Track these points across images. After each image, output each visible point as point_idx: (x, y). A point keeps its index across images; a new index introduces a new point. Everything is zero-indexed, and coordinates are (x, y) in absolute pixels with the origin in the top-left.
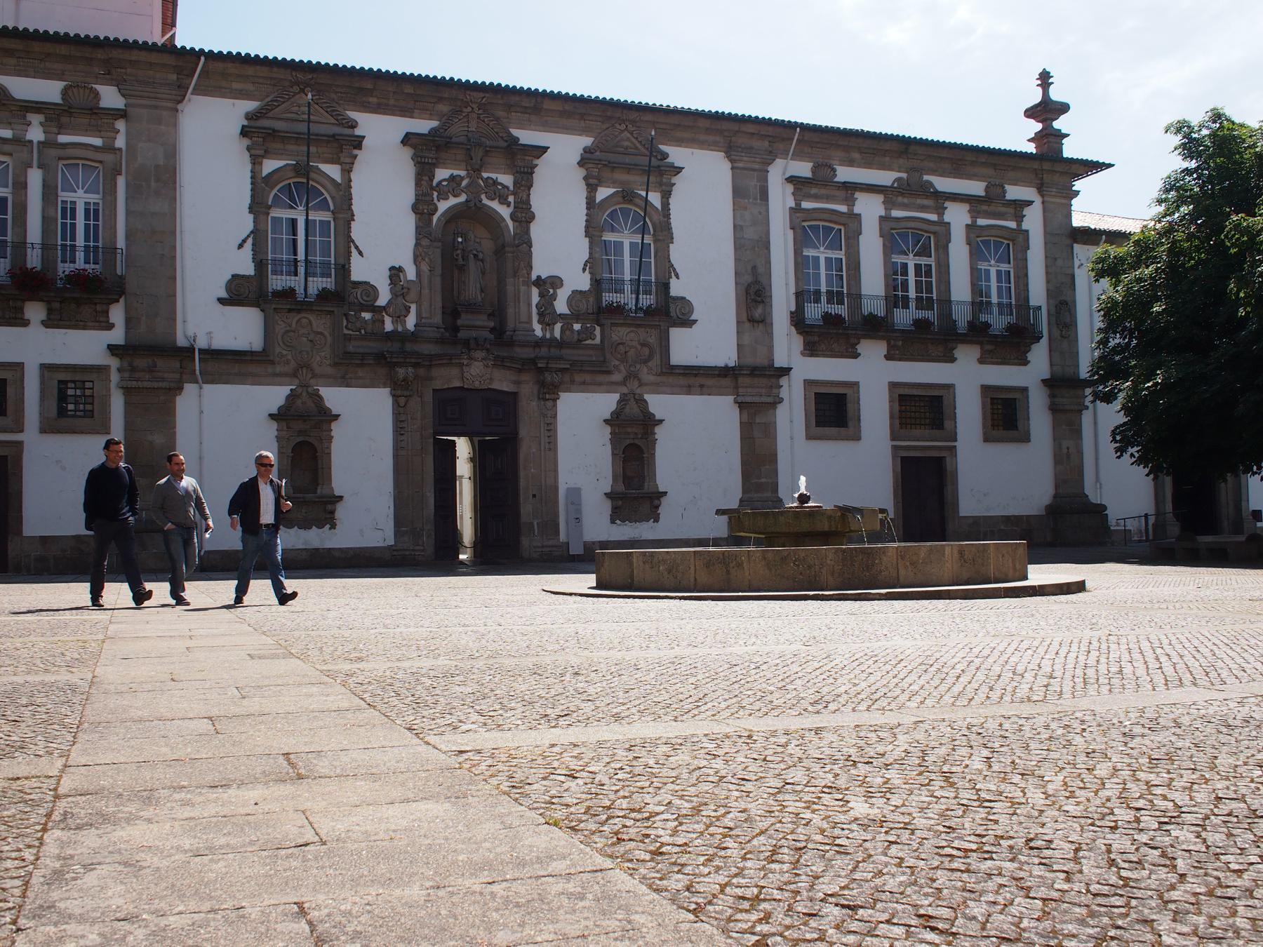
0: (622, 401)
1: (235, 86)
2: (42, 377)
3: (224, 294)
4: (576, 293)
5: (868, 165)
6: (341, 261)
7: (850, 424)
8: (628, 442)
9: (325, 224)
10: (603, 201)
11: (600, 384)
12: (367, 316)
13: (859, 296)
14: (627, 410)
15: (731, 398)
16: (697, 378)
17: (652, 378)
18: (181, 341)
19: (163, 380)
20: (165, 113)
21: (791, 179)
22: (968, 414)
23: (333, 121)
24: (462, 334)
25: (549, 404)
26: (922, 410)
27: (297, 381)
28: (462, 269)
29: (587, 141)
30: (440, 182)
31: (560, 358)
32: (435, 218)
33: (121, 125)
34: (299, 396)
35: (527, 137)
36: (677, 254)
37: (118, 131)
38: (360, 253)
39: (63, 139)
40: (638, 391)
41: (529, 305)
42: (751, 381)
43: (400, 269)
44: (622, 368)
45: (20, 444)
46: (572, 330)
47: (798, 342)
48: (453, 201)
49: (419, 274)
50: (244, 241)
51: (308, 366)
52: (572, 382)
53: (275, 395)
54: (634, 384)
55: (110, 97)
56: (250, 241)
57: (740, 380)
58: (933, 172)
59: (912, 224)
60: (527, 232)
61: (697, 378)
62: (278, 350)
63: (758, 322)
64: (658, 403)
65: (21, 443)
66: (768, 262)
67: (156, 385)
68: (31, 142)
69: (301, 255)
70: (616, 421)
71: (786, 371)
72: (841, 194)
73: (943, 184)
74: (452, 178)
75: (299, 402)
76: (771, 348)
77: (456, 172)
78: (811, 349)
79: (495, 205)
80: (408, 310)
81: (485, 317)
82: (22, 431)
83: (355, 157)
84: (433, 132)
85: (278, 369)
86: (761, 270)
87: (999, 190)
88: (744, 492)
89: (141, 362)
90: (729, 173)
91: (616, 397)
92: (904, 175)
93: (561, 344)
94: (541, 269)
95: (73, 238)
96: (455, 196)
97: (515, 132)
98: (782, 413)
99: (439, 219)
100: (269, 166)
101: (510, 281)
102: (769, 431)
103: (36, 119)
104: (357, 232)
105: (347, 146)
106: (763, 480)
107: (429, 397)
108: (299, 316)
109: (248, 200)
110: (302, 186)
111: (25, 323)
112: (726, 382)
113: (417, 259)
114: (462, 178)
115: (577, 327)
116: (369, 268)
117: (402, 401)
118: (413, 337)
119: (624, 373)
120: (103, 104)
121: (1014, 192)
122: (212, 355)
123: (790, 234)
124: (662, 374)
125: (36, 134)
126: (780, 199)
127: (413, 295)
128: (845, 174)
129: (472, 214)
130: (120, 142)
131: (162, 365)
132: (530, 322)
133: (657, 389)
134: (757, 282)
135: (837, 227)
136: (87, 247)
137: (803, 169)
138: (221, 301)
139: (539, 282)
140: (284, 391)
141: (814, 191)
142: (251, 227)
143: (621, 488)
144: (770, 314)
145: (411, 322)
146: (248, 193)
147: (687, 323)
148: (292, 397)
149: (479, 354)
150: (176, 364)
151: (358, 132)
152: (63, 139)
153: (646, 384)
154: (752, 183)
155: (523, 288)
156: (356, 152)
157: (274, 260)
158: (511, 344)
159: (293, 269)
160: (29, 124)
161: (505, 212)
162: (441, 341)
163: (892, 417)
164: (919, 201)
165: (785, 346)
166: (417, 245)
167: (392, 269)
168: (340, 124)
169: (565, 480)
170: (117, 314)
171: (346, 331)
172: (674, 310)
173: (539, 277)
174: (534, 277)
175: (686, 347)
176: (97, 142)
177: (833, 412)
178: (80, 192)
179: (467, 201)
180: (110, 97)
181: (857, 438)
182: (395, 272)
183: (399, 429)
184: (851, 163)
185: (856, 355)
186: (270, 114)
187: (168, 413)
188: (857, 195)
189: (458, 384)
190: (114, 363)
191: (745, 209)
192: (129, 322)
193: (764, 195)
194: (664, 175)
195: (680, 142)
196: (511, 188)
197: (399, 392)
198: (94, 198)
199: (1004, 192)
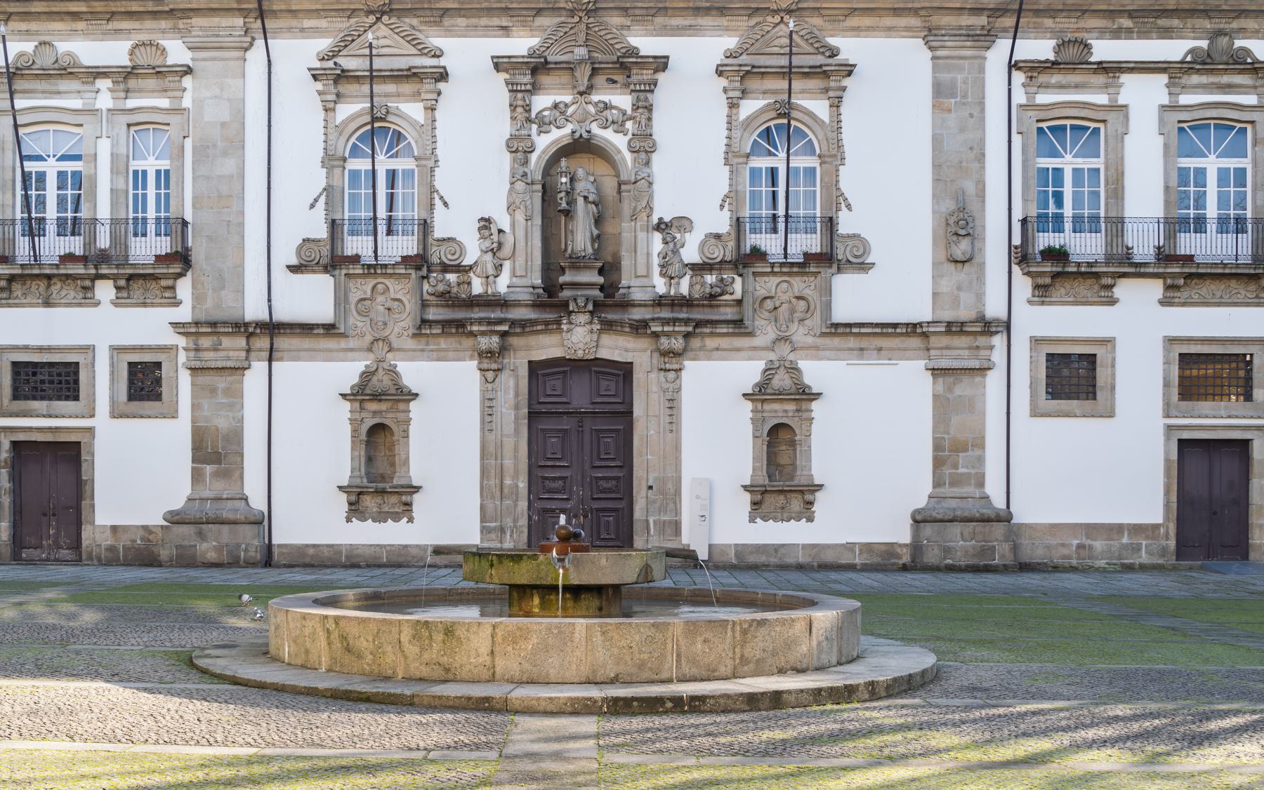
0: (769, 372)
1: (307, 23)
2: (112, 358)
3: (294, 261)
4: (709, 236)
5: (1144, 34)
6: (424, 215)
8: (776, 421)
9: (409, 174)
10: (748, 118)
11: (738, 350)
12: (452, 277)
13: (1121, 221)
15: (921, 364)
17: (810, 340)
19: (228, 358)
20: (231, 63)
23: (415, 51)
24: (566, 294)
25: (672, 375)
27: (372, 356)
28: (568, 213)
29: (731, 42)
32: (534, 157)
33: (187, 82)
34: (373, 373)
35: (647, 44)
36: (848, 180)
37: (185, 90)
38: (446, 204)
39: (131, 103)
40: (792, 357)
41: (648, 254)
42: (954, 341)
43: (488, 220)
44: (769, 328)
45: (91, 430)
46: (703, 284)
47: (1023, 286)
48: (555, 134)
50: (316, 200)
52: (702, 348)
54: (784, 349)
55: (177, 52)
56: (323, 199)
57: (933, 339)
59: (1214, 113)
60: (648, 163)
62: (351, 321)
63: (963, 262)
64: (814, 371)
65: (91, 430)
69: (382, 213)
72: (1101, 79)
74: (556, 106)
75: (375, 379)
76: (980, 296)
77: (559, 98)
78: (1042, 292)
80: (499, 268)
82: (93, 416)
83: (439, 93)
85: (352, 343)
89: (205, 342)
90: (928, 65)
91: (760, 365)
93: (685, 302)
94: (663, 209)
95: (144, 210)
96: (558, 128)
97: (634, 41)
98: (994, 381)
99: (539, 157)
102: (974, 406)
104: (442, 181)
107: (524, 371)
108: (375, 281)
109: (321, 154)
111: (98, 304)
112: (915, 342)
113: (511, 208)
114: (566, 106)
115: (710, 279)
116: (456, 224)
117: (490, 375)
120: (170, 61)
124: (823, 334)
125: (105, 101)
127: (507, 250)
128: (1104, 49)
129: (580, 147)
130: (187, 102)
132: (648, 275)
133: (815, 352)
134: (962, 209)
135: (1093, 125)
136: (158, 219)
137: (1039, 48)
139: (661, 226)
142: (323, 185)
143: (763, 479)
148: (367, 375)
151: (442, 62)
152: (131, 103)
153: (802, 348)
155: (642, 236)
156: (441, 86)
157: (352, 220)
158: (626, 305)
159: (371, 227)
161: (618, 141)
162: (537, 305)
163: (1167, 384)
164: (1225, 79)
166: (511, 191)
167: (482, 219)
168: (422, 53)
169: (692, 468)
170: (184, 288)
172: (840, 253)
173: (660, 219)
174: (655, 221)
176: (164, 103)
177: (1073, 378)
178: (151, 160)
179: (573, 132)
181: (1111, 414)
182: (486, 223)
184: (1117, 34)
185: (1112, 302)
186: (344, 52)
188: (1125, 78)
189: (556, 353)
190: (181, 342)
192: (198, 298)
194: (832, 74)
195: (857, 31)
196: (629, 112)
197: (485, 366)
198: (164, 164)
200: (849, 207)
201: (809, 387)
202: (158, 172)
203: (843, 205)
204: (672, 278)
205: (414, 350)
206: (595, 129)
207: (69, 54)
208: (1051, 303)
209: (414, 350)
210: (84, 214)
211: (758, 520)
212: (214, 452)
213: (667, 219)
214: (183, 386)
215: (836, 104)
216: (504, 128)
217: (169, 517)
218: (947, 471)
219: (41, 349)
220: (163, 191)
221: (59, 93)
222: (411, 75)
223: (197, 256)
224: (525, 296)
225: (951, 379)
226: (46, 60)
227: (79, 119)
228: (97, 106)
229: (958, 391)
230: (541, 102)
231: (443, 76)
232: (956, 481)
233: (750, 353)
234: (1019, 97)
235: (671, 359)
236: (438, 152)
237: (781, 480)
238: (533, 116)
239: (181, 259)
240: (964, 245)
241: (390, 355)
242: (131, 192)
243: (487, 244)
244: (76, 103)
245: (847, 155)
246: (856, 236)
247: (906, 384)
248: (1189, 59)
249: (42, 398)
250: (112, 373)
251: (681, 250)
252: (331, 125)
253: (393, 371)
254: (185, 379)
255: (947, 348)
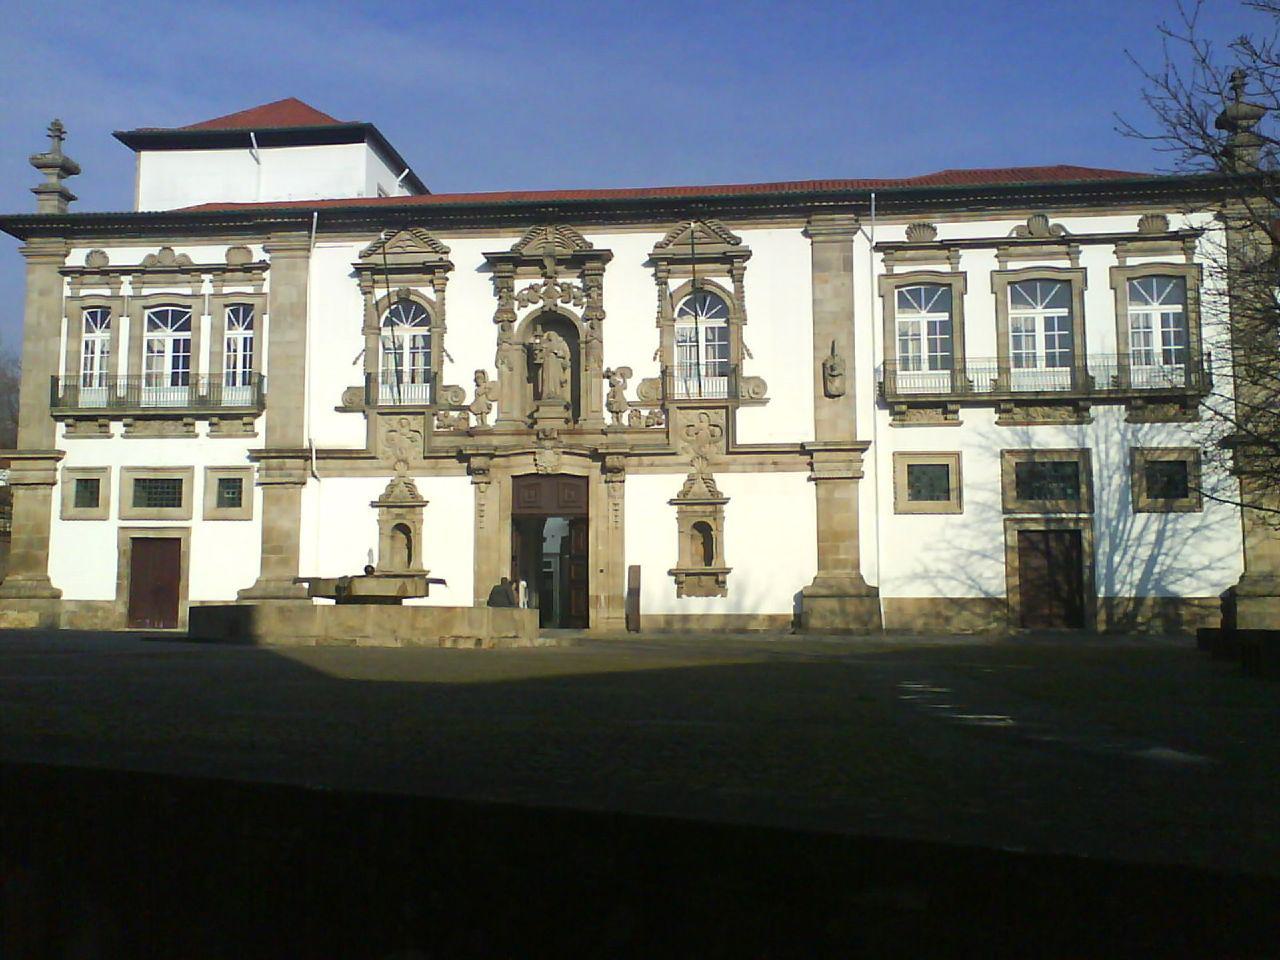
0: (691, 479)
3: (340, 404)
7: (953, 495)
11: (667, 465)
12: (455, 414)
14: (695, 488)
16: (769, 456)
18: (306, 445)
19: (290, 475)
20: (298, 260)
21: (879, 247)
22: (1109, 479)
26: (1040, 480)
30: (521, 292)
31: (623, 444)
32: (516, 325)
33: (267, 275)
36: (751, 335)
38: (451, 360)
43: (483, 372)
48: (532, 307)
49: (500, 375)
50: (357, 359)
51: (405, 461)
52: (640, 465)
53: (377, 486)
55: (258, 253)
56: (362, 358)
58: (1066, 213)
61: (769, 456)
64: (725, 482)
65: (187, 529)
66: (851, 334)
67: (287, 480)
68: (203, 295)
70: (680, 501)
71: (863, 447)
73: (1077, 224)
74: (531, 287)
76: (853, 422)
77: (534, 281)
79: (570, 306)
80: (489, 408)
81: (562, 408)
84: (516, 246)
85: (382, 463)
86: (842, 342)
87: (1159, 223)
88: (821, 565)
89: (275, 462)
91: (684, 477)
92: (1025, 223)
94: (611, 361)
97: (588, 238)
98: (865, 487)
99: (520, 325)
100: (380, 293)
101: (583, 374)
103: (207, 277)
105: (438, 269)
106: (842, 557)
107: (508, 483)
110: (408, 308)
111: (197, 436)
113: (501, 359)
116: (457, 374)
118: (489, 432)
119: (692, 454)
121: (1177, 221)
122: (326, 455)
123: (879, 302)
125: (207, 288)
126: (867, 268)
128: (947, 230)
130: (266, 288)
131: (291, 461)
133: (724, 468)
138: (337, 409)
139: (608, 375)
140: (387, 481)
141: (910, 254)
142: (363, 347)
144: (853, 387)
145: (491, 420)
146: (362, 318)
147: (759, 400)
148: (392, 486)
149: (547, 443)
150: (300, 462)
154: (833, 254)
156: (449, 275)
160: (202, 281)
161: (579, 312)
165: (870, 421)
170: (260, 424)
171: (436, 430)
172: (745, 390)
173: (608, 370)
174: (604, 369)
175: (751, 427)
176: (250, 290)
180: (258, 253)
182: (480, 376)
183: (480, 512)
187: (295, 504)
189: (533, 470)
191: (826, 282)
193: (848, 265)
199: (1167, 224)
200: (750, 356)
201: (722, 494)
202: (245, 339)
203: (746, 355)
204: (617, 413)
205: (424, 468)
206: (559, 302)
207: (184, 256)
208: (909, 426)
209: (424, 468)
210: (191, 371)
211: (684, 596)
212: (278, 547)
213: (613, 369)
214: (256, 497)
215: (738, 280)
216: (493, 304)
217: (242, 594)
218: (830, 557)
219: (155, 469)
220: (248, 353)
221: (176, 283)
222: (427, 269)
223: (268, 402)
224: (509, 427)
225: (830, 486)
226: (167, 261)
227: (188, 302)
228: (202, 292)
229: (837, 495)
230: (520, 285)
231: (449, 267)
232: (839, 564)
233: (677, 468)
234: (881, 269)
235: (613, 473)
236: (446, 322)
237: (703, 566)
238: (516, 292)
239: (260, 404)
240: (837, 382)
241: (409, 472)
242: (225, 354)
243: (481, 390)
244: (187, 291)
245: (748, 318)
246: (757, 378)
247: (795, 491)
248: (1014, 235)
249: (155, 506)
250: (206, 487)
251: (624, 392)
252: (369, 305)
253: (410, 486)
254: (258, 492)
255: (826, 462)
